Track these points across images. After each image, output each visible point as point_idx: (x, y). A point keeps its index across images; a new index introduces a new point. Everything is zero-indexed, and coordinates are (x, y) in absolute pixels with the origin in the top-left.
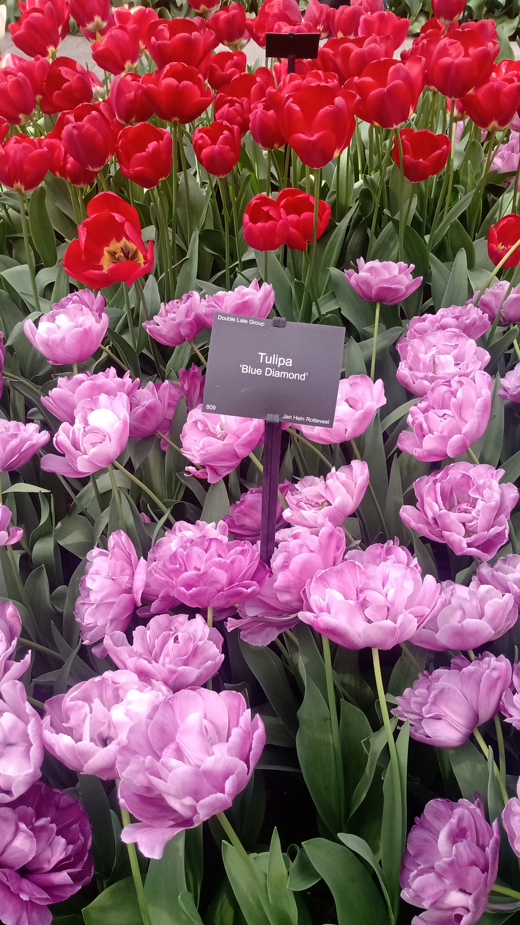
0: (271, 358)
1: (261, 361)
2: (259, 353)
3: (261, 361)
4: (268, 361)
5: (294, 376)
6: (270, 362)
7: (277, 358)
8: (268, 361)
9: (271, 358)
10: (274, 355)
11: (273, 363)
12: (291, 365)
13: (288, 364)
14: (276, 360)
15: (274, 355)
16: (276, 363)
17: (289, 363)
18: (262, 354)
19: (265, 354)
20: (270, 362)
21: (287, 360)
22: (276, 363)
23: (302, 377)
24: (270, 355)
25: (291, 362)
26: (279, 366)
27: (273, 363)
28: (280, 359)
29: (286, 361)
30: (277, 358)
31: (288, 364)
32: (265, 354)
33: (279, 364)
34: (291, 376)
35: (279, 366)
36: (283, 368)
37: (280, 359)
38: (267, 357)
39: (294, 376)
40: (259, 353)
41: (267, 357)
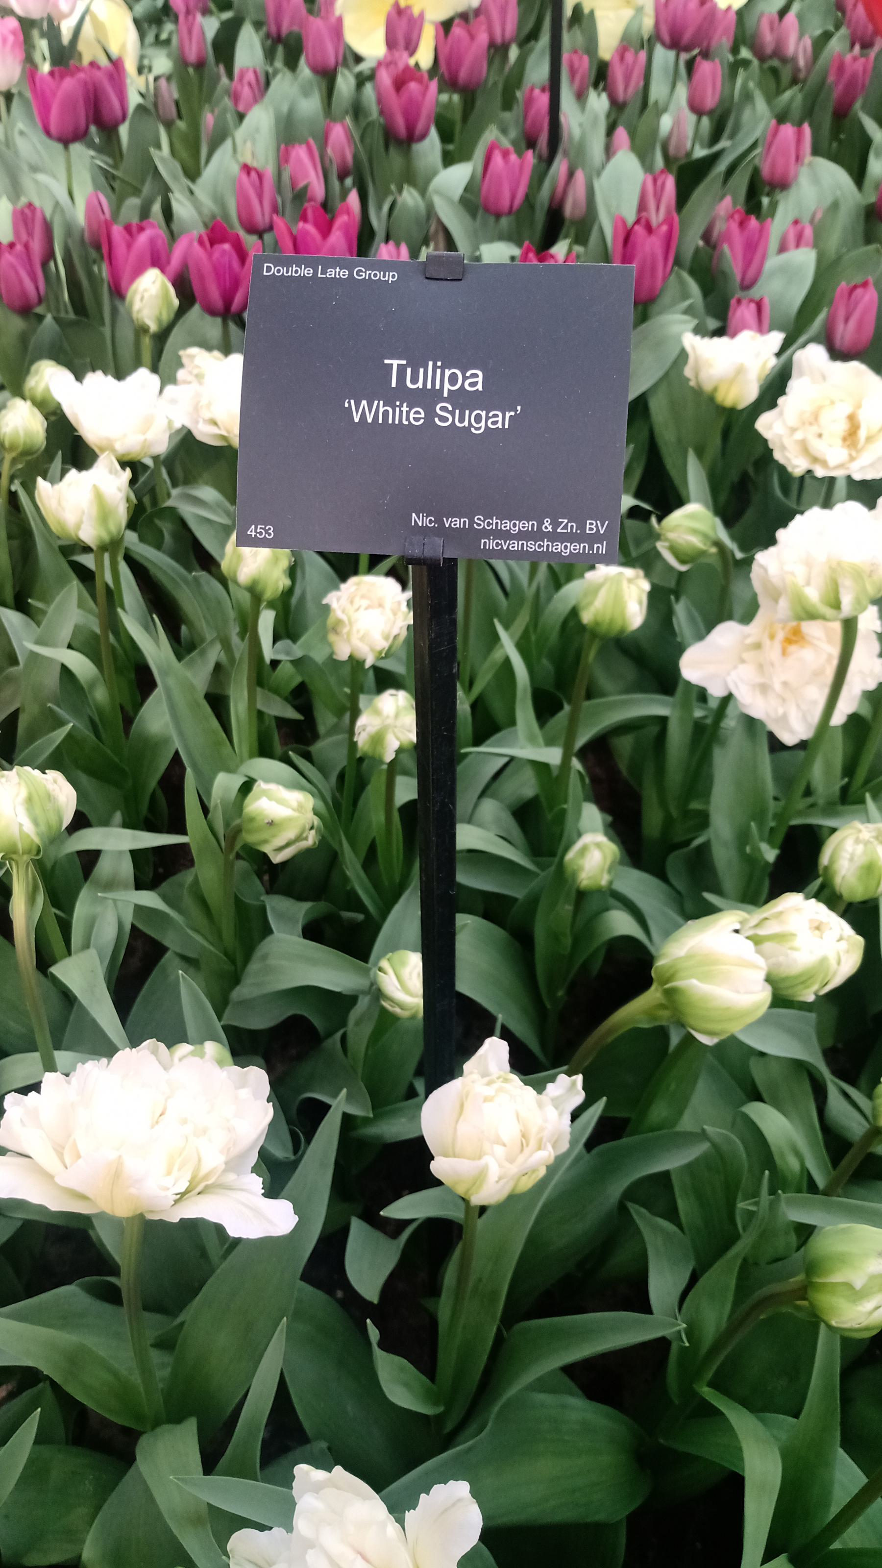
0: (422, 370)
1: (394, 385)
2: (387, 361)
3: (394, 385)
4: (414, 380)
6: (420, 385)
7: (439, 371)
8: (414, 380)
9: (422, 370)
10: (431, 363)
11: (429, 387)
12: (480, 387)
13: (471, 385)
14: (434, 376)
15: (431, 363)
16: (438, 387)
17: (475, 380)
18: (395, 363)
19: (404, 362)
20: (420, 385)
21: (468, 374)
22: (438, 387)
24: (417, 363)
25: (480, 379)
26: (446, 395)
27: (429, 387)
29: (465, 378)
30: (439, 371)
31: (471, 385)
32: (404, 362)
33: (447, 386)
35: (446, 395)
37: (448, 373)
38: (409, 370)
40: (387, 361)
41: (409, 370)
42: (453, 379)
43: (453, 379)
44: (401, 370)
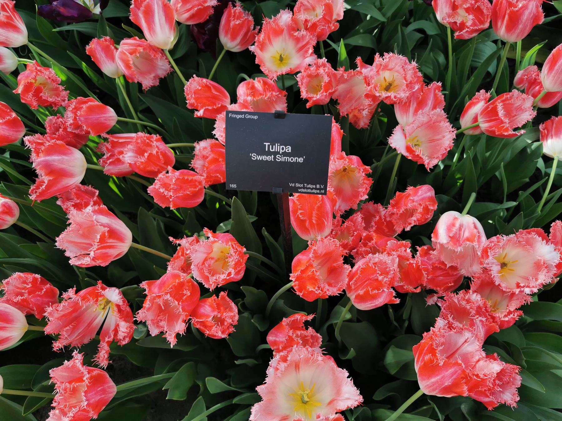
4: (272, 149)
5: (294, 160)
6: (274, 150)
8: (272, 149)
12: (290, 151)
14: (277, 148)
17: (289, 149)
18: (267, 144)
23: (301, 160)
24: (273, 144)
25: (290, 149)
28: (281, 147)
33: (281, 151)
34: (292, 160)
36: (285, 154)
39: (294, 160)
42: (283, 149)
43: (283, 149)
44: (269, 146)
